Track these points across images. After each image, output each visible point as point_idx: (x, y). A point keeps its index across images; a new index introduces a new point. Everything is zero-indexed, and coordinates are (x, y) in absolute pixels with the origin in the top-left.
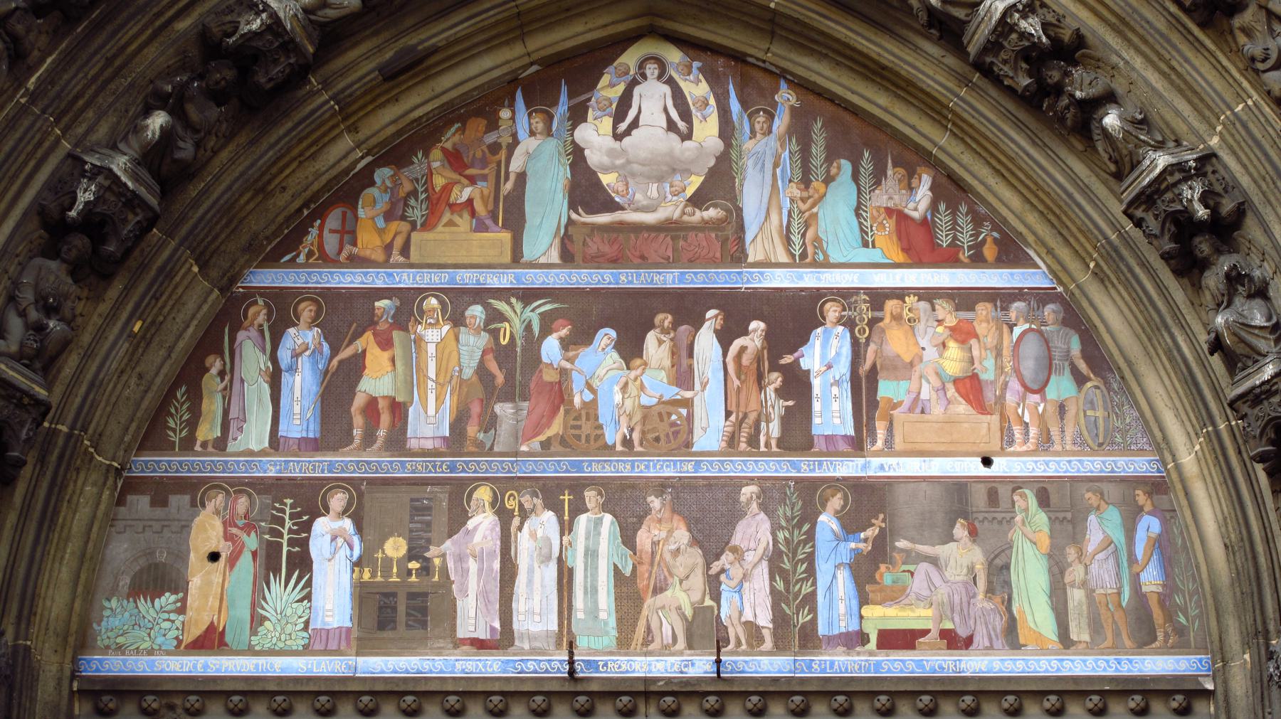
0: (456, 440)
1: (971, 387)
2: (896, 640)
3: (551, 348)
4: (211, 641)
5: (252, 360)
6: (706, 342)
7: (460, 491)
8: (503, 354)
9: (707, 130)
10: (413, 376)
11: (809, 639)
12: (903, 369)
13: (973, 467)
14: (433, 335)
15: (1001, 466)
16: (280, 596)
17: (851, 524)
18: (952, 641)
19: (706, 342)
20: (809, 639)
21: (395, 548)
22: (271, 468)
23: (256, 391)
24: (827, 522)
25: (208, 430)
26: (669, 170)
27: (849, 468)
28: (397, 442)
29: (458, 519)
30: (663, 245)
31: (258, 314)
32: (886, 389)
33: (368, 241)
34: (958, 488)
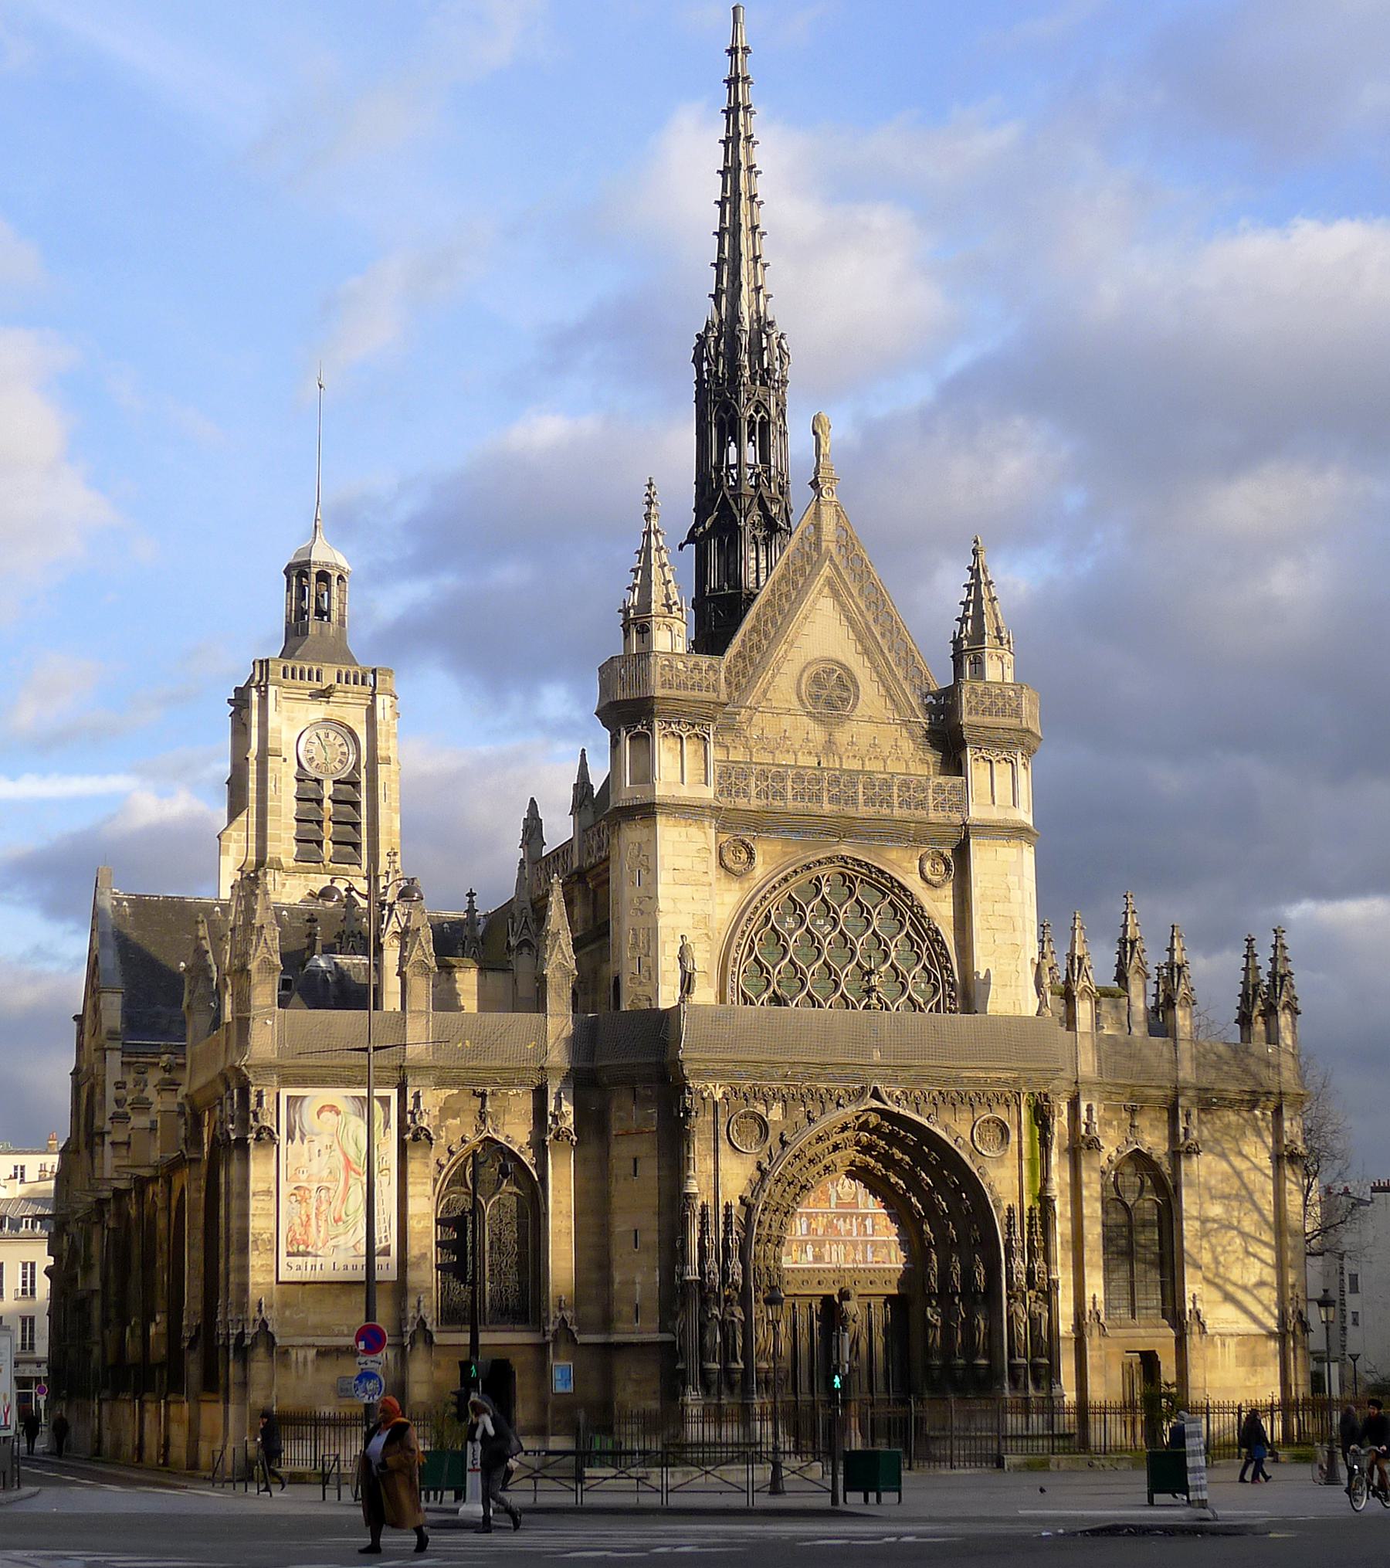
0: (824, 1234)
1: (886, 1226)
2: (876, 1262)
3: (835, 1221)
4: (796, 1262)
5: (798, 1222)
6: (854, 1220)
7: (825, 1241)
8: (828, 1221)
9: (854, 1187)
10: (818, 1225)
11: (867, 1262)
12: (878, 1224)
13: (886, 1238)
14: (820, 1219)
15: (890, 1238)
16: (804, 1256)
17: (872, 1246)
18: (884, 1262)
19: (854, 1220)
20: (867, 1262)
21: (817, 1249)
22: (801, 1238)
23: (799, 1227)
24: (869, 1246)
25: (793, 1233)
26: (850, 1194)
27: (871, 1238)
28: (817, 1234)
29: (825, 1245)
30: (848, 1206)
31: (798, 1215)
32: (876, 1227)
33: (811, 1205)
34: (884, 1241)
